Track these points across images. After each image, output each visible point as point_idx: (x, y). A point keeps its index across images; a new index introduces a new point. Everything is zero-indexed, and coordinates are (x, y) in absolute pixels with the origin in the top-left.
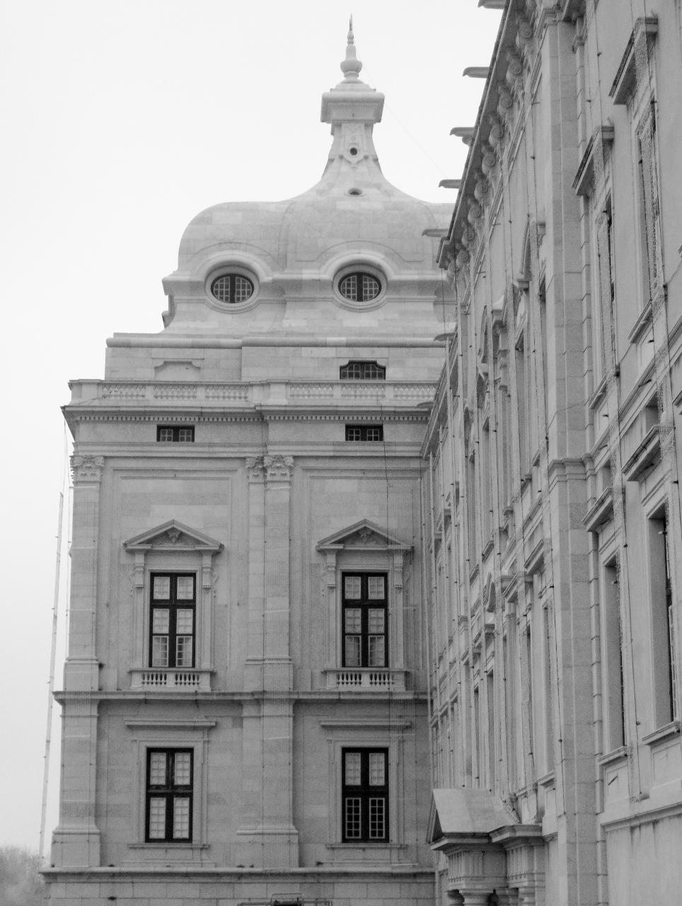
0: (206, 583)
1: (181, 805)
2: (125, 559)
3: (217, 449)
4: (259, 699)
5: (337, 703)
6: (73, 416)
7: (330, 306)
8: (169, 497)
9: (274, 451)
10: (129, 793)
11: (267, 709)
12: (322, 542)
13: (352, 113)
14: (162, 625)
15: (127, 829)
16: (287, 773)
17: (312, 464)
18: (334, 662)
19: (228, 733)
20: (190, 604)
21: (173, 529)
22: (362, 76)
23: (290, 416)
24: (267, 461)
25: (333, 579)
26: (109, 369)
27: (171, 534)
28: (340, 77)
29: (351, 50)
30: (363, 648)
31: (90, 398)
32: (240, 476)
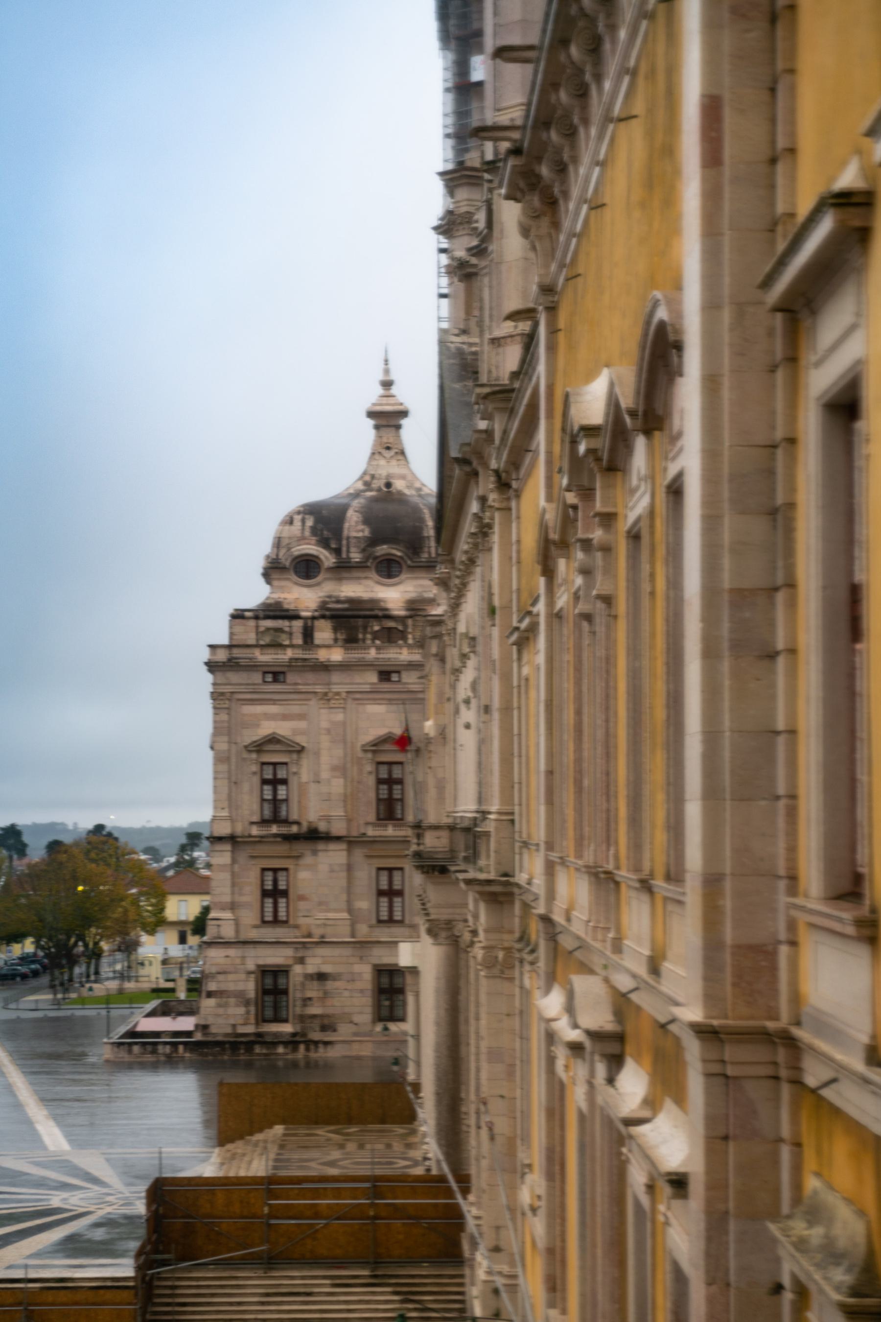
0: (295, 770)
1: (282, 902)
2: (245, 755)
3: (300, 687)
4: (328, 838)
5: (373, 842)
6: (212, 666)
7: (370, 583)
8: (268, 720)
9: (335, 688)
10: (250, 894)
11: (332, 846)
12: (363, 746)
13: (388, 420)
14: (268, 795)
15: (250, 917)
16: (344, 883)
17: (358, 696)
18: (372, 817)
19: (308, 859)
20: (284, 782)
21: (274, 738)
22: (394, 390)
23: (343, 667)
24: (330, 695)
25: (369, 768)
26: (232, 634)
27: (273, 739)
28: (380, 391)
29: (387, 371)
30: (389, 810)
31: (222, 656)
32: (313, 703)
